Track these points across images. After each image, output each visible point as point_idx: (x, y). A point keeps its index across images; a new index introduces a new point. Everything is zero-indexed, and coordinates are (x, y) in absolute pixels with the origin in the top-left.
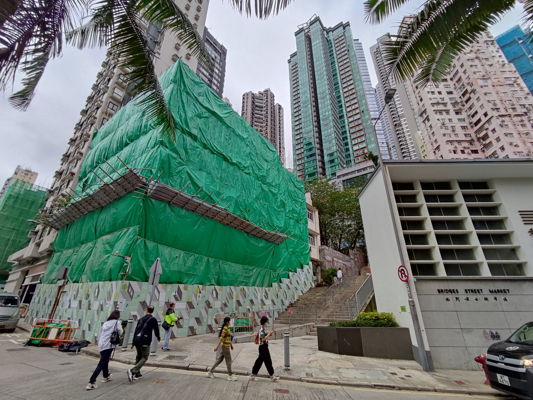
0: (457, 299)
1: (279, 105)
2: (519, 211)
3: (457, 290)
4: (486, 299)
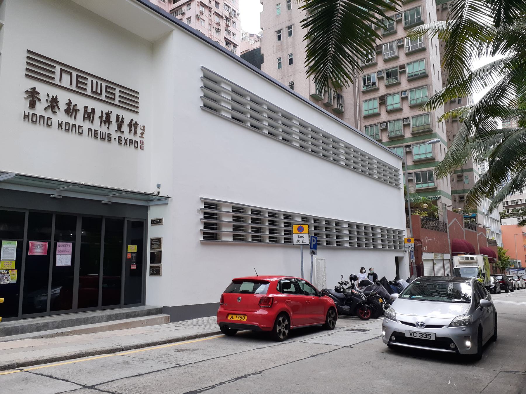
2: (28, 51)
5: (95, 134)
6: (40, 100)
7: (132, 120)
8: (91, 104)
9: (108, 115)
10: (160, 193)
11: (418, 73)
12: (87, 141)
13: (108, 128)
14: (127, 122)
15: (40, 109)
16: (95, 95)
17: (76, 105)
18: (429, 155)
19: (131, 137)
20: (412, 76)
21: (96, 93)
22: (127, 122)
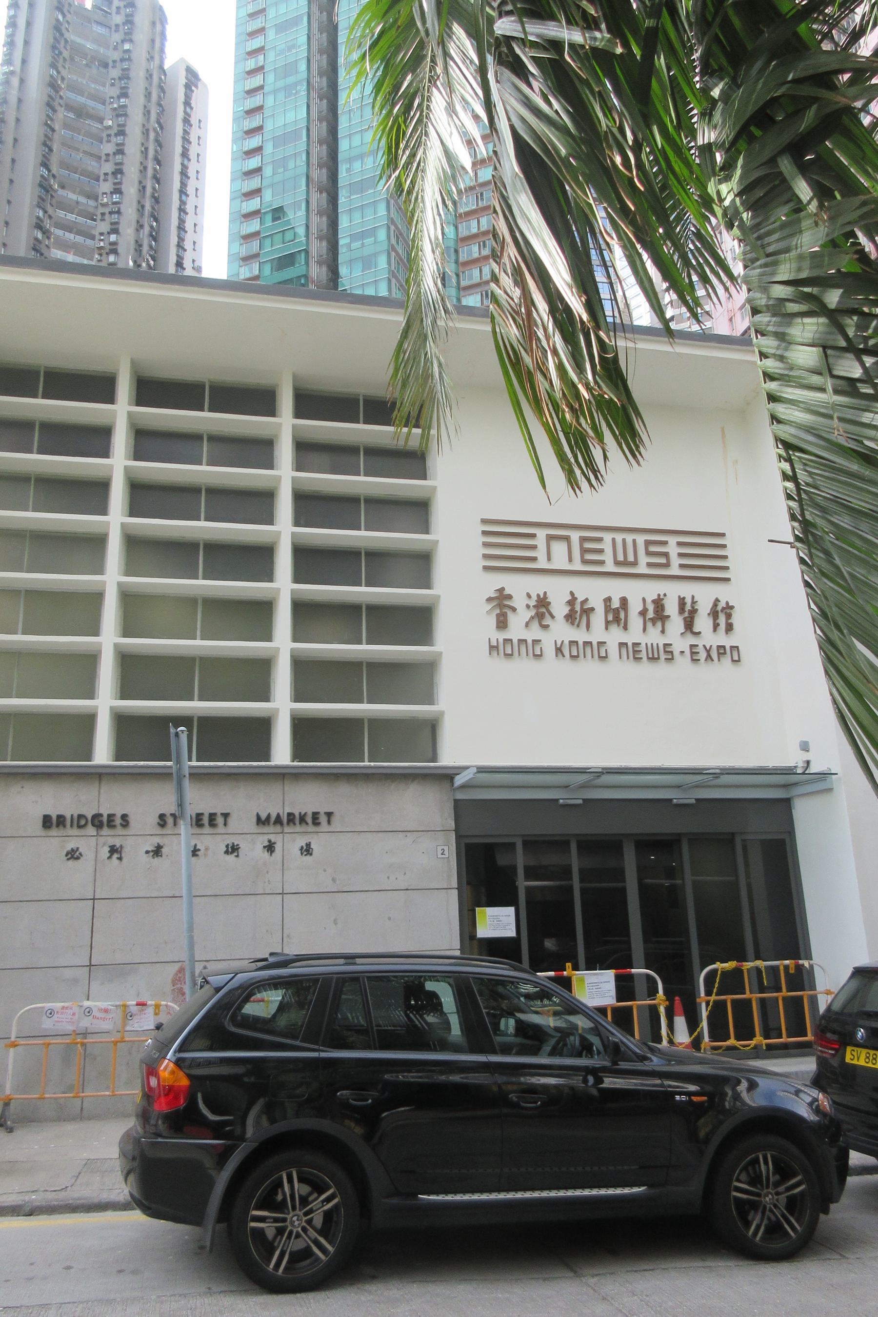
0: (113, 850)
1: (190, 71)
2: (484, 521)
3: (124, 817)
4: (233, 849)
5: (634, 652)
6: (514, 610)
7: (717, 600)
8: (616, 589)
9: (659, 604)
10: (812, 764)
12: (621, 669)
13: (663, 632)
14: (704, 608)
15: (519, 626)
16: (625, 569)
17: (587, 599)
19: (722, 639)
21: (625, 563)
22: (704, 608)
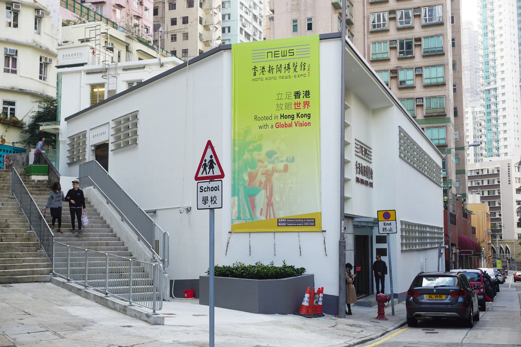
11: (434, 49)
18: (442, 142)
20: (428, 52)
